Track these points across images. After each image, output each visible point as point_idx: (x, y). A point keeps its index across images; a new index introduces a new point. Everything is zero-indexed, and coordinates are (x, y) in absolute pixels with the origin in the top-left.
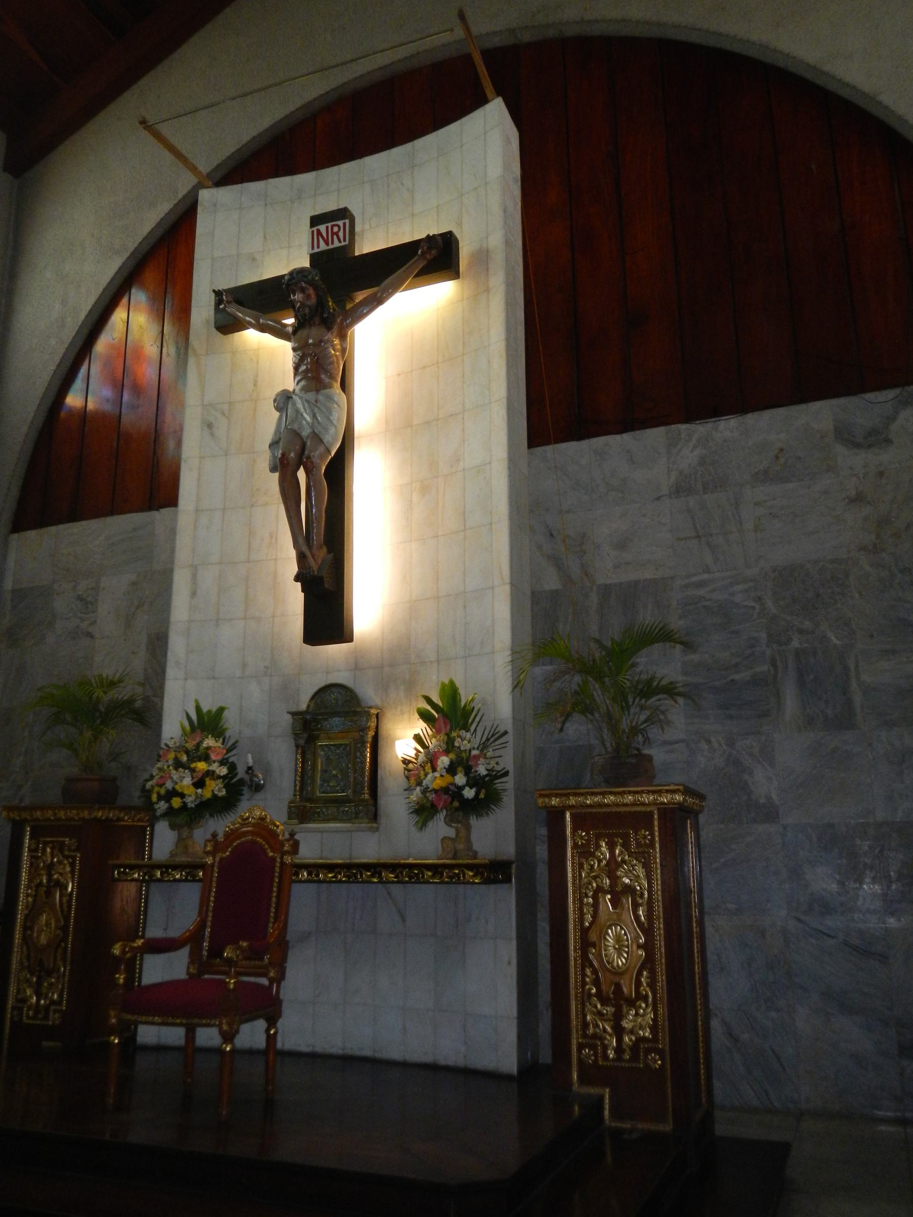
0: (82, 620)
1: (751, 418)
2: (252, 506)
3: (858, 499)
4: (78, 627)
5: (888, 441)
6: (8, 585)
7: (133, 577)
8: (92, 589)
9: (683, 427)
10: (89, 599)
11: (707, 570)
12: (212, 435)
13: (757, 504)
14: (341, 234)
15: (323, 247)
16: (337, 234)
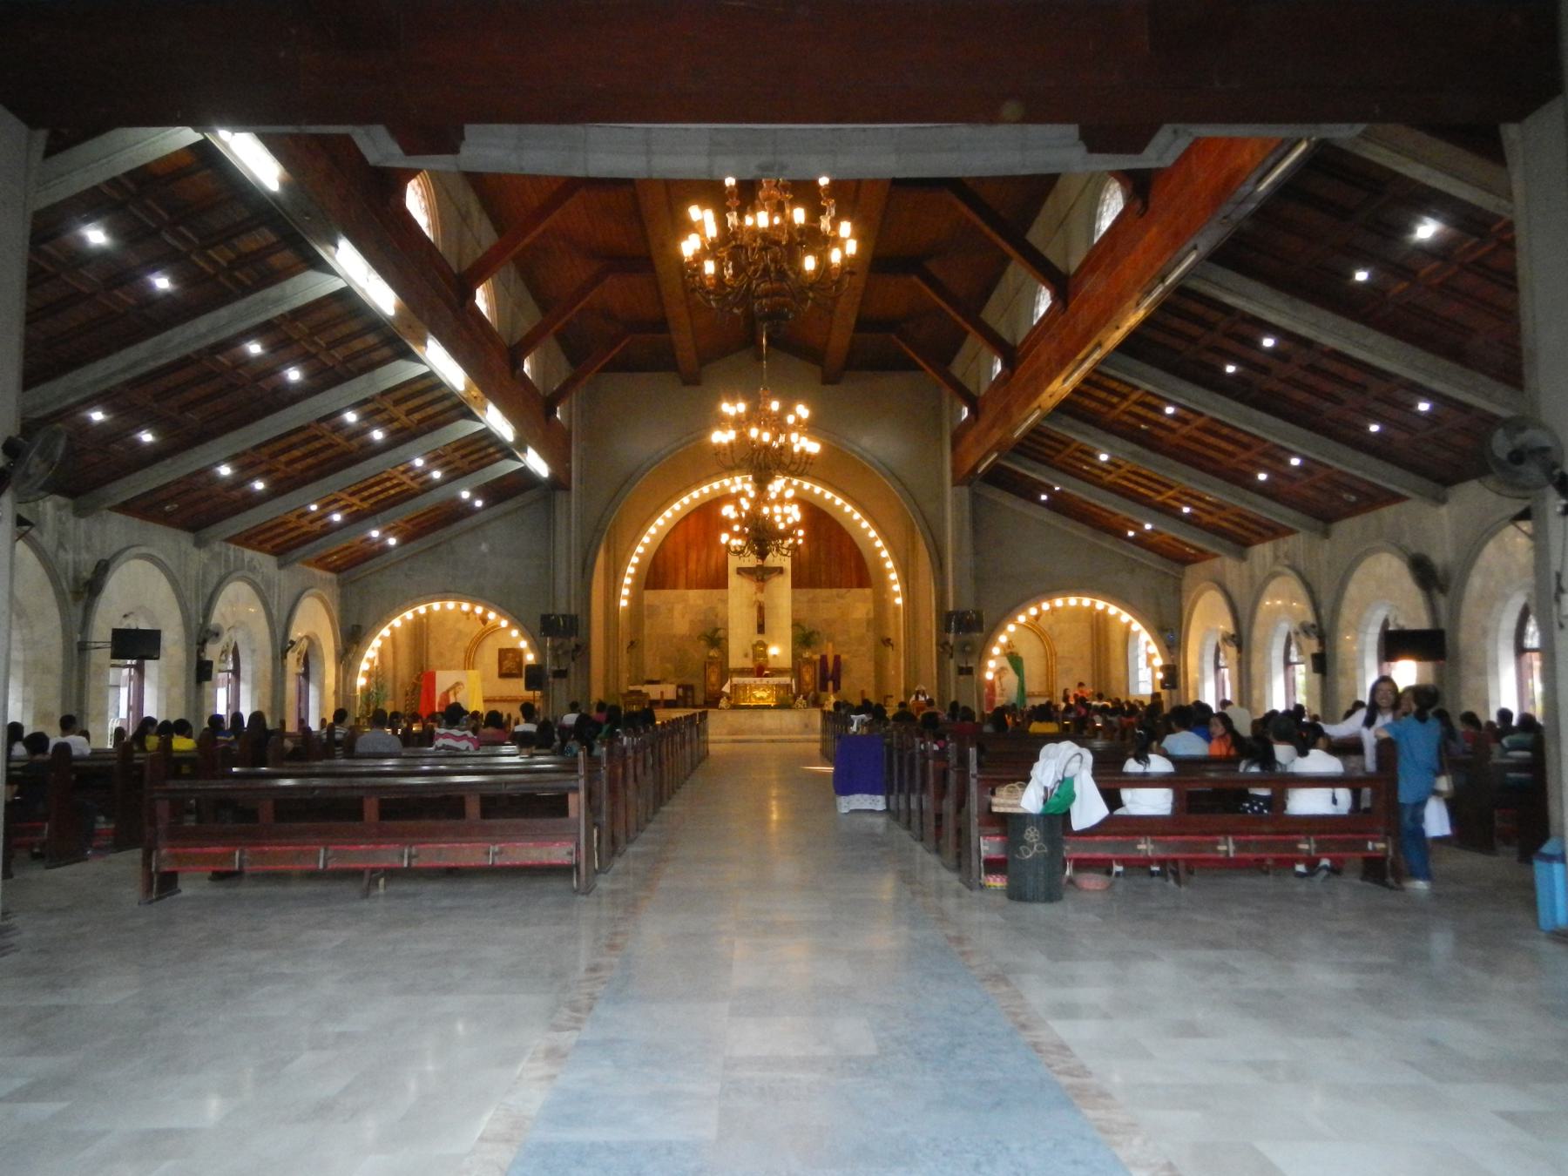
6: (645, 602)
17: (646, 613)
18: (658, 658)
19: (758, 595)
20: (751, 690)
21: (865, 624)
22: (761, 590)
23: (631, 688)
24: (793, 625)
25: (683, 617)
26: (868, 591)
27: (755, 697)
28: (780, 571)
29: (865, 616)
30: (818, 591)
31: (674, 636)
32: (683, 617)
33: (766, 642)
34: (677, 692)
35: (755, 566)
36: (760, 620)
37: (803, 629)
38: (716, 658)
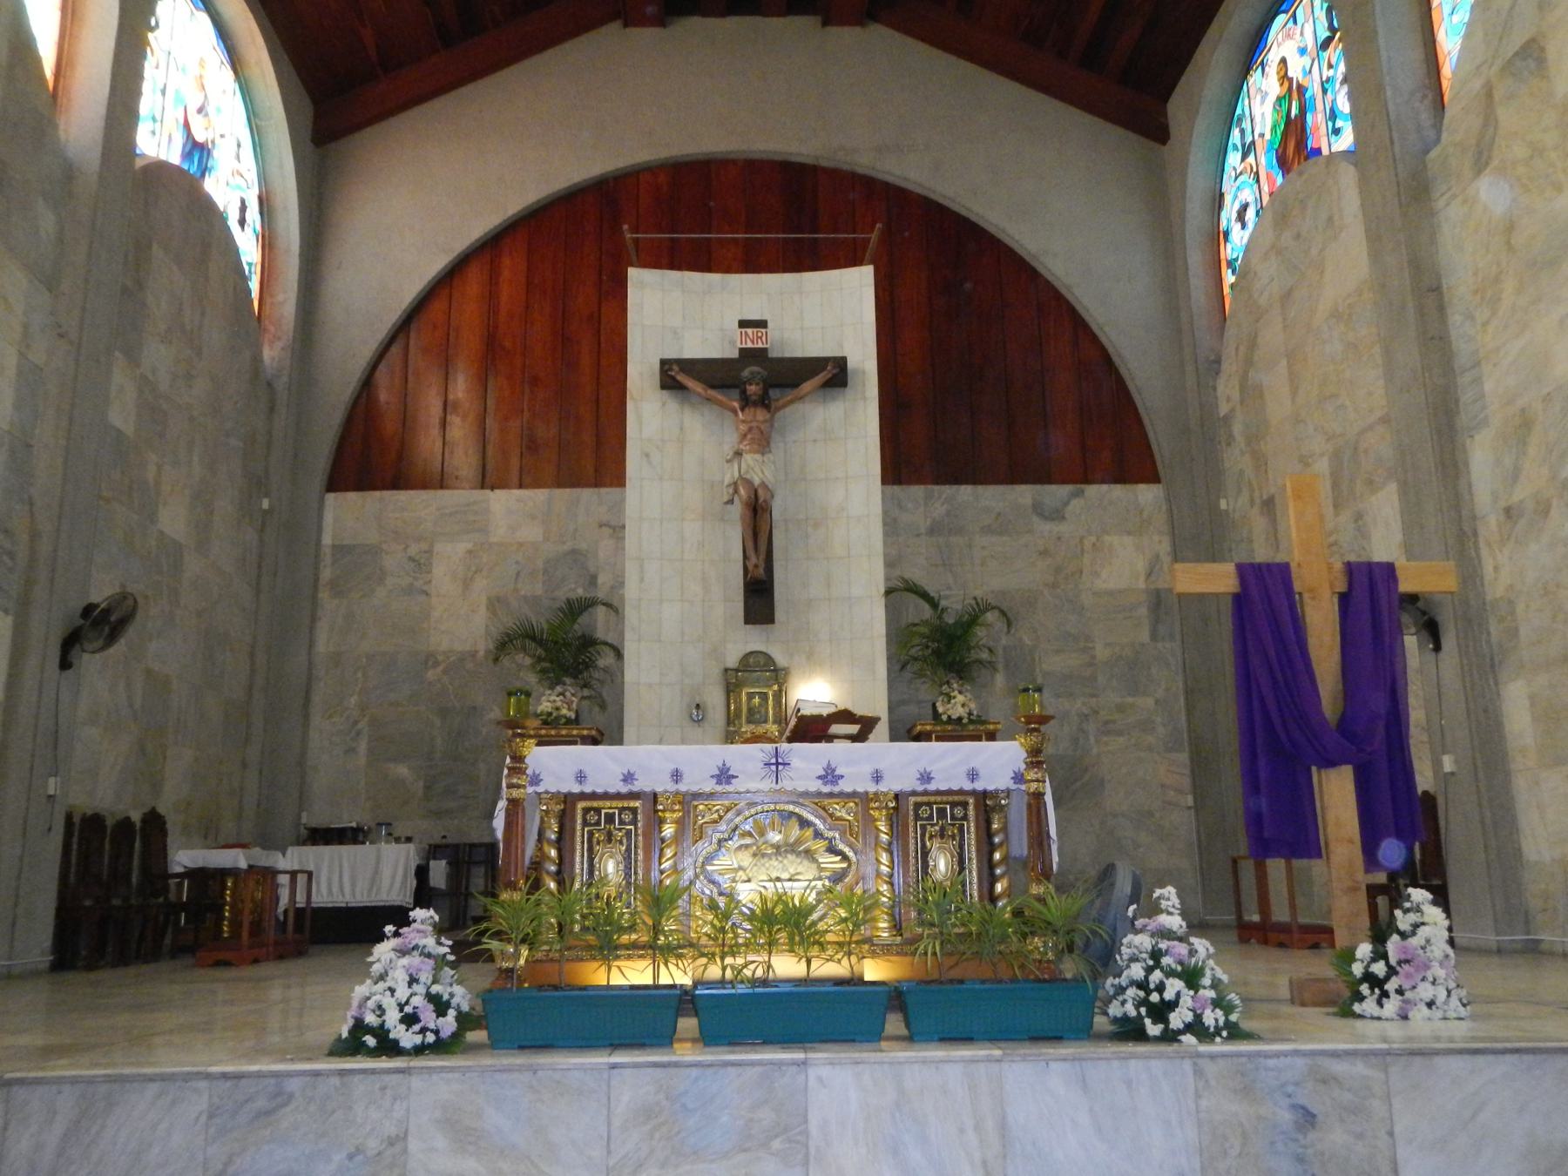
0: (416, 579)
1: (980, 488)
2: (683, 520)
3: (1044, 553)
4: (412, 584)
5: (1063, 518)
6: (327, 540)
7: (470, 546)
8: (425, 552)
9: (936, 488)
10: (422, 561)
11: (949, 588)
12: (650, 463)
13: (983, 548)
14: (764, 338)
15: (750, 345)
16: (761, 338)
17: (326, 574)
18: (363, 746)
19: (749, 459)
20: (689, 829)
21: (1143, 611)
22: (763, 443)
23: (183, 858)
24: (889, 592)
25: (467, 584)
26: (1147, 495)
27: (723, 909)
28: (835, 374)
29: (1142, 585)
30: (965, 492)
31: (430, 660)
32: (467, 584)
33: (781, 660)
34: (422, 873)
35: (735, 354)
36: (761, 571)
37: (934, 604)
38: (569, 721)
